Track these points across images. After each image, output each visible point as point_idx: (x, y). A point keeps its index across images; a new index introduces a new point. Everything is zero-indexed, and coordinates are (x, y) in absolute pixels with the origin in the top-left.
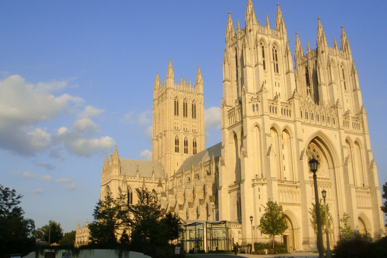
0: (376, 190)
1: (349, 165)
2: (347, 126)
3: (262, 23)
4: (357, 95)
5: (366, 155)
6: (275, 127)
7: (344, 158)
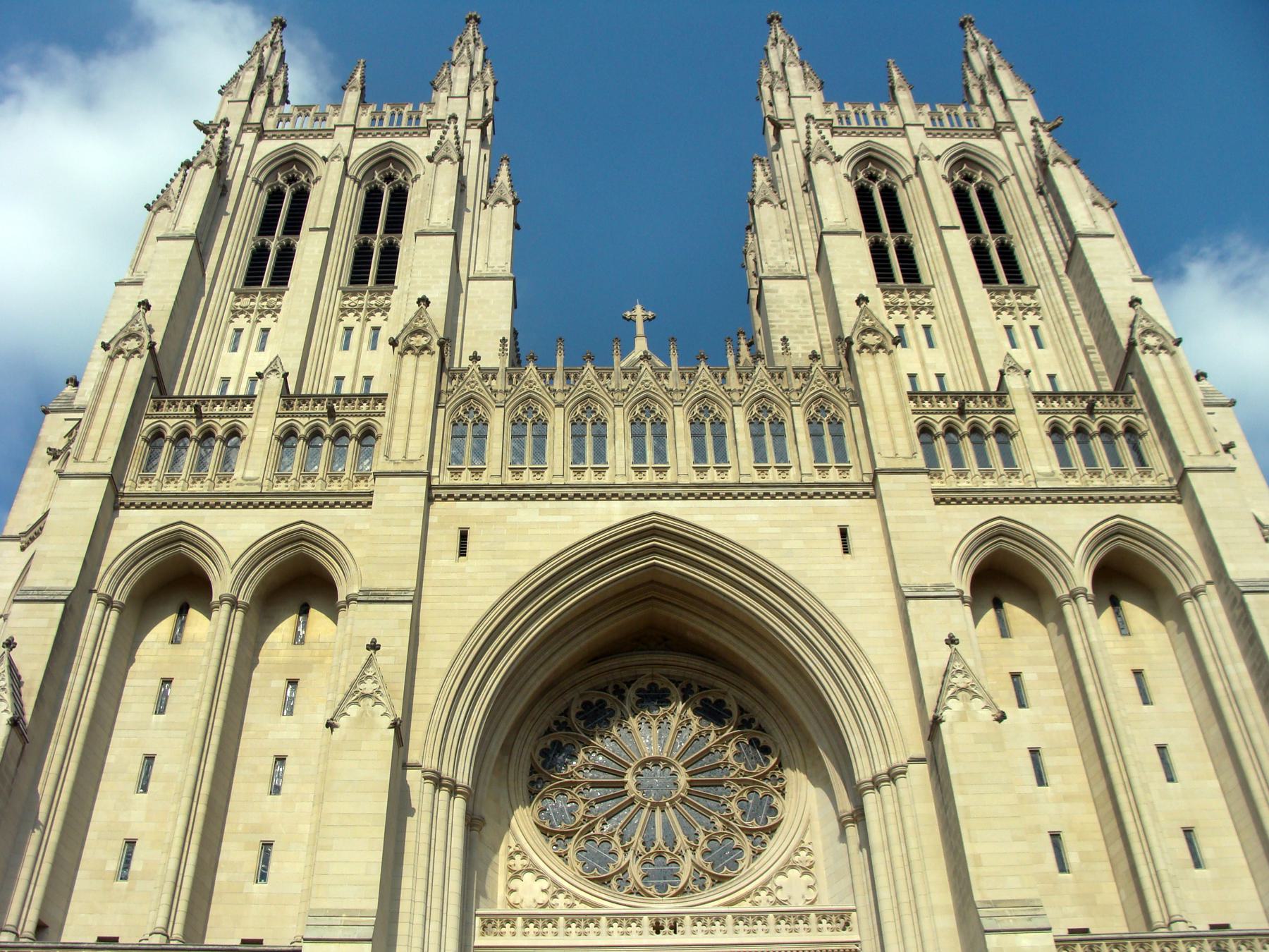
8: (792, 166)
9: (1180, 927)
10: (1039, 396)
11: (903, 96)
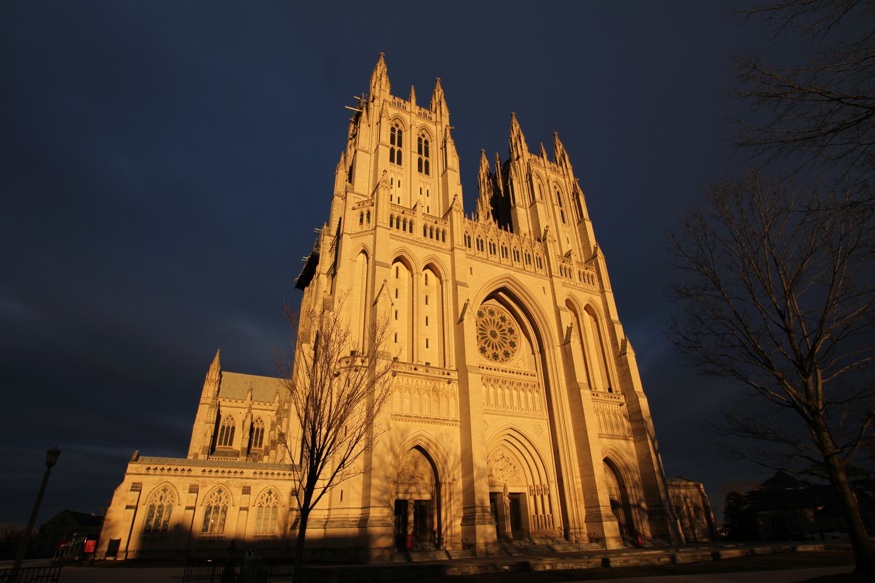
0: (638, 397)
1: (574, 342)
2: (569, 276)
3: (399, 91)
4: (585, 229)
5: (609, 331)
6: (405, 256)
7: (562, 331)
8: (375, 114)
9: (420, 363)
10: (424, 214)
11: (413, 101)
